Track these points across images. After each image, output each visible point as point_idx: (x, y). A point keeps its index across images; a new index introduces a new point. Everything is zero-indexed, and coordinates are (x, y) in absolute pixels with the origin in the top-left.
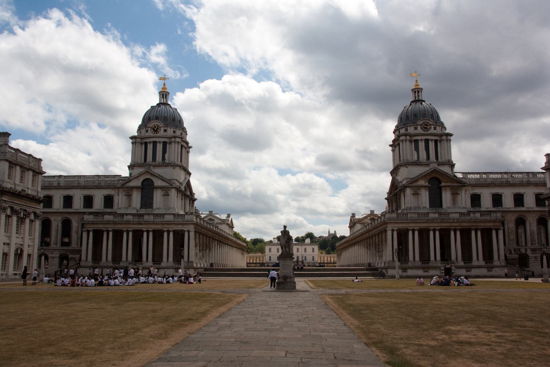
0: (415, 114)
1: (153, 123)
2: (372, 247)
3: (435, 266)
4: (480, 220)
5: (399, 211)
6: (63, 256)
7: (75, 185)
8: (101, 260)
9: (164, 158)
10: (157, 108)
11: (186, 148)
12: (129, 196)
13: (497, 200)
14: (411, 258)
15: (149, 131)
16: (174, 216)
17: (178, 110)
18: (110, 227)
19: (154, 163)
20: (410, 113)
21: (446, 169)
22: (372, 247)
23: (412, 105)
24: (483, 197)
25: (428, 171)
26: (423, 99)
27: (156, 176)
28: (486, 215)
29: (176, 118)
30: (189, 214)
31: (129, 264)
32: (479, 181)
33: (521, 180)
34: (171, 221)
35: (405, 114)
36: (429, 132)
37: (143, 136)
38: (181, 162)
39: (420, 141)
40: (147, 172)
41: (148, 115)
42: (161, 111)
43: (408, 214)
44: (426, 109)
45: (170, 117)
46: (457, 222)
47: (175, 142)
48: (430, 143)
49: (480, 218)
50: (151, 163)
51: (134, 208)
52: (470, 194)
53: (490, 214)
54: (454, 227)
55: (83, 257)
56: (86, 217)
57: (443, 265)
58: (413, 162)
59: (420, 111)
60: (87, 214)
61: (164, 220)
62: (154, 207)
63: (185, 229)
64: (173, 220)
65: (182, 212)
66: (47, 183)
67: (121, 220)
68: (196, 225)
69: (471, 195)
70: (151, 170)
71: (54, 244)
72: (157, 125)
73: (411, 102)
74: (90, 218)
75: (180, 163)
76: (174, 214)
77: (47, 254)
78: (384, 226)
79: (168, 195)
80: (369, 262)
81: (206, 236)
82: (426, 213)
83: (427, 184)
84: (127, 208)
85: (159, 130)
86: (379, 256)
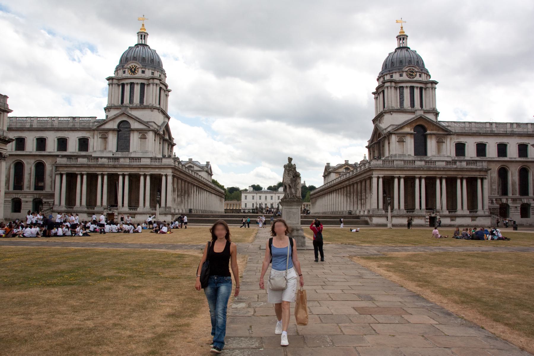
0: (401, 61)
1: (131, 64)
2: (352, 194)
3: (420, 215)
4: (466, 169)
6: (36, 200)
7: (48, 127)
8: (75, 205)
10: (135, 48)
11: (165, 91)
12: (105, 138)
13: (481, 149)
14: (396, 206)
15: (126, 72)
16: (151, 160)
17: (157, 52)
18: (85, 171)
19: (131, 105)
20: (395, 59)
21: (431, 117)
22: (352, 194)
23: (397, 52)
24: (468, 146)
25: (414, 118)
26: (408, 46)
27: (133, 118)
28: (472, 164)
29: (155, 59)
30: (167, 158)
31: (104, 209)
32: (464, 129)
33: (505, 130)
34: (147, 165)
35: (390, 60)
36: (415, 79)
37: (120, 77)
38: (159, 104)
39: (405, 88)
40: (124, 114)
41: (126, 56)
42: (139, 51)
43: (395, 161)
44: (412, 56)
45: (148, 58)
46: (443, 171)
47: (153, 84)
48: (415, 90)
49: (466, 167)
50: (128, 105)
51: (110, 151)
52: (455, 143)
53: (476, 163)
54: (440, 176)
55: (57, 202)
56: (60, 161)
57: (428, 214)
58: (397, 110)
59: (405, 57)
60: (60, 157)
61: (141, 164)
62: (131, 150)
63: (162, 173)
64: (150, 164)
66: (19, 124)
67: (95, 163)
68: (174, 169)
69: (456, 144)
70: (128, 113)
71: (27, 188)
72: (135, 66)
73: (396, 49)
74: (64, 161)
75: (158, 106)
77: (20, 198)
78: (369, 174)
79: (146, 138)
80: (348, 209)
81: (185, 181)
82: (412, 160)
83: (412, 131)
84: (102, 151)
85: (137, 71)
86: (361, 204)
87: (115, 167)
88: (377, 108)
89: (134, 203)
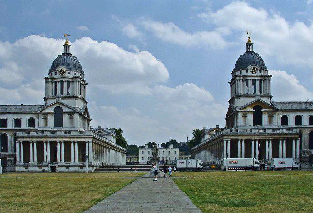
5: (233, 128)
8: (29, 161)
9: (68, 94)
12: (46, 119)
13: (298, 120)
18: (35, 140)
21: (265, 100)
55: (18, 159)
56: (18, 134)
62: (63, 126)
65: (82, 130)
76: (77, 131)
83: (252, 110)
87: (54, 137)
88: (231, 94)
89: (68, 158)
